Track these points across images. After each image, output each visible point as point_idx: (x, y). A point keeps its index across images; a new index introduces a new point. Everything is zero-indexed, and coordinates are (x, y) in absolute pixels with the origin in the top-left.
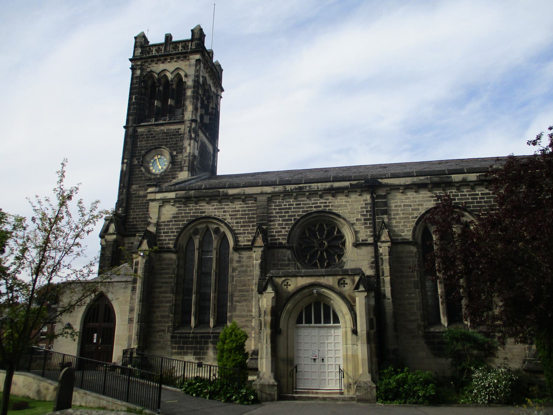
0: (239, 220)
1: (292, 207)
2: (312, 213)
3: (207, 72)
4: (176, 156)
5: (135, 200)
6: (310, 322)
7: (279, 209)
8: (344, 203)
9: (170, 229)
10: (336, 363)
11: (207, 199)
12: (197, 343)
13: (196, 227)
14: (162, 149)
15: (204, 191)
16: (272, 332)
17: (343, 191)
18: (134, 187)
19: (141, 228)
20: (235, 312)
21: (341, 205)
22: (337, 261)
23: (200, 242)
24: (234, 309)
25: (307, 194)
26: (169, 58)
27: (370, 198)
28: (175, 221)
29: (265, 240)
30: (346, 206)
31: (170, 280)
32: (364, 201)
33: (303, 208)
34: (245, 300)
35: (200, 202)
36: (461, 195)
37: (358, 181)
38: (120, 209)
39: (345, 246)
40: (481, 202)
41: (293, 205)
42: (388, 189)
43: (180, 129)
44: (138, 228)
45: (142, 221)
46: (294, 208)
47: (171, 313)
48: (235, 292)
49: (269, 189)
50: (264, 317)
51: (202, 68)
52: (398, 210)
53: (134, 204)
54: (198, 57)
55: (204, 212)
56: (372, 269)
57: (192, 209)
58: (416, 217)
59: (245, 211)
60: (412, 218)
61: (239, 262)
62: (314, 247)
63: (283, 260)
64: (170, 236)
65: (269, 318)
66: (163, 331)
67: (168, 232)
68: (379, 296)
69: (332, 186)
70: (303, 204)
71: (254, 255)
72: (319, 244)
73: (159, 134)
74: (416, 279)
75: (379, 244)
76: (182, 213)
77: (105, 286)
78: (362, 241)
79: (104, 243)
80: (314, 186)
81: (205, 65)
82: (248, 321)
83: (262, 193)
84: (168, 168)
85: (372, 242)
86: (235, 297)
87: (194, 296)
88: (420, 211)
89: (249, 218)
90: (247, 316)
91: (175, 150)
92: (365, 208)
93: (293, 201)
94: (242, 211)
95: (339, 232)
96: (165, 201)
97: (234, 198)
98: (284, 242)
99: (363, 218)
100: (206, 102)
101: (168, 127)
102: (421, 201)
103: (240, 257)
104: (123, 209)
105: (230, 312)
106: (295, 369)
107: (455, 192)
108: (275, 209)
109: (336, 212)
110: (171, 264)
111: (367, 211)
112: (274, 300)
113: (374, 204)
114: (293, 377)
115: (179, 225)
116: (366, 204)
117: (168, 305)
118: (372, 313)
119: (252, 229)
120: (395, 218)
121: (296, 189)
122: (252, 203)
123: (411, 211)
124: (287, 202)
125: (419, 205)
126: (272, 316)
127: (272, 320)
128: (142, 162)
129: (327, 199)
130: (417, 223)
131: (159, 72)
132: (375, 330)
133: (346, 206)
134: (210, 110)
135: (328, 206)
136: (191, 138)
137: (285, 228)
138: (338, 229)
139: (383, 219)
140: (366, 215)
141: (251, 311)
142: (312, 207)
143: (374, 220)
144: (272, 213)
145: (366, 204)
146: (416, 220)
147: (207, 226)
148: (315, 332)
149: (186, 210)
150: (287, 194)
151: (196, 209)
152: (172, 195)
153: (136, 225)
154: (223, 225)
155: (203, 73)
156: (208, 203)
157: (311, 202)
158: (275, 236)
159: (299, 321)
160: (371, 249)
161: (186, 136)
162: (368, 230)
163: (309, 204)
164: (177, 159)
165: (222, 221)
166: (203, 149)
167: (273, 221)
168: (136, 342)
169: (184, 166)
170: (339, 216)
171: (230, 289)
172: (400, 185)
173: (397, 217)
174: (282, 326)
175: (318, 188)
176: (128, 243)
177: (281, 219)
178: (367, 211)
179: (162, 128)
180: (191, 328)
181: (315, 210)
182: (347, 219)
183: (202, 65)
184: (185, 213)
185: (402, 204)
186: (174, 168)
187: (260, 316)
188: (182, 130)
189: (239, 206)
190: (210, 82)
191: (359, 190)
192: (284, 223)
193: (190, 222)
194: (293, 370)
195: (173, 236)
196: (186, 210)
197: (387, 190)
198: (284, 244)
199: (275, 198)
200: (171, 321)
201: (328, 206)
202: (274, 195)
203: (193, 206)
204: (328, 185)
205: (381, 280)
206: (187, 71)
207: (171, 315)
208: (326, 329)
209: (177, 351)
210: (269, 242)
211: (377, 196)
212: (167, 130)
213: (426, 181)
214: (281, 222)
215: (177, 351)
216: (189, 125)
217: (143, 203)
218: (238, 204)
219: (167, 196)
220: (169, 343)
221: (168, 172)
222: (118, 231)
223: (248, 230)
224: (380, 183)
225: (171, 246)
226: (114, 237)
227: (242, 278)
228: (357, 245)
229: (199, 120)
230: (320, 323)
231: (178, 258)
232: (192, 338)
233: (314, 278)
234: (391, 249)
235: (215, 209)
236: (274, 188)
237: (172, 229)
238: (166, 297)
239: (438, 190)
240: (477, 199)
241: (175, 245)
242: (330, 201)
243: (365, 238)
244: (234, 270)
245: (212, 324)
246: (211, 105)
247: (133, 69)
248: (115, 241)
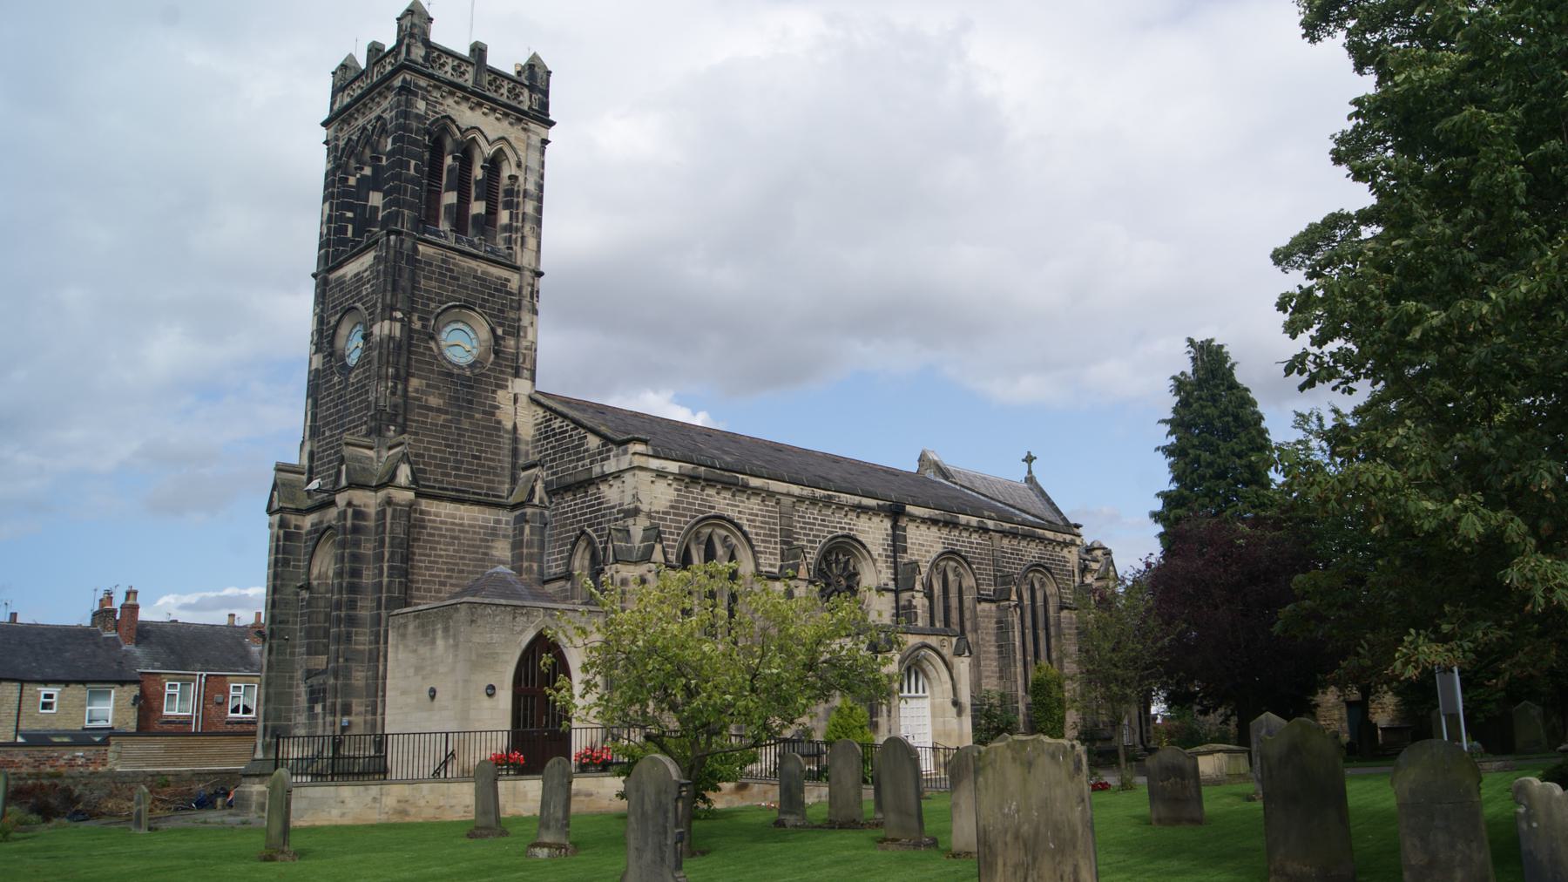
4: (503, 339)
5: (420, 415)
11: (719, 486)
14: (473, 314)
15: (718, 471)
18: (414, 382)
19: (435, 480)
26: (487, 104)
28: (675, 514)
33: (828, 527)
38: (392, 428)
41: (816, 519)
43: (508, 280)
44: (429, 480)
45: (437, 466)
46: (819, 525)
49: (796, 489)
53: (417, 421)
55: (713, 508)
57: (696, 499)
59: (764, 516)
73: (465, 275)
76: (682, 502)
77: (551, 616)
83: (788, 495)
89: (770, 529)
91: (501, 325)
92: (887, 540)
94: (764, 516)
96: (661, 474)
97: (756, 492)
99: (884, 553)
101: (485, 266)
104: (398, 429)
108: (799, 522)
109: (864, 541)
111: (888, 545)
115: (680, 522)
116: (887, 535)
121: (825, 497)
122: (772, 506)
129: (851, 519)
131: (464, 127)
142: (836, 527)
144: (795, 527)
145: (887, 535)
149: (688, 497)
150: (814, 501)
152: (673, 467)
153: (424, 471)
156: (718, 493)
163: (833, 522)
164: (504, 347)
165: (739, 527)
167: (797, 539)
169: (523, 368)
172: (919, 517)
178: (888, 545)
179: (473, 264)
184: (688, 503)
186: (500, 365)
202: (801, 499)
203: (698, 493)
206: (522, 154)
212: (483, 273)
216: (531, 282)
217: (436, 425)
223: (769, 548)
228: (881, 590)
235: (728, 505)
237: (670, 527)
243: (886, 581)
248: (411, 505)
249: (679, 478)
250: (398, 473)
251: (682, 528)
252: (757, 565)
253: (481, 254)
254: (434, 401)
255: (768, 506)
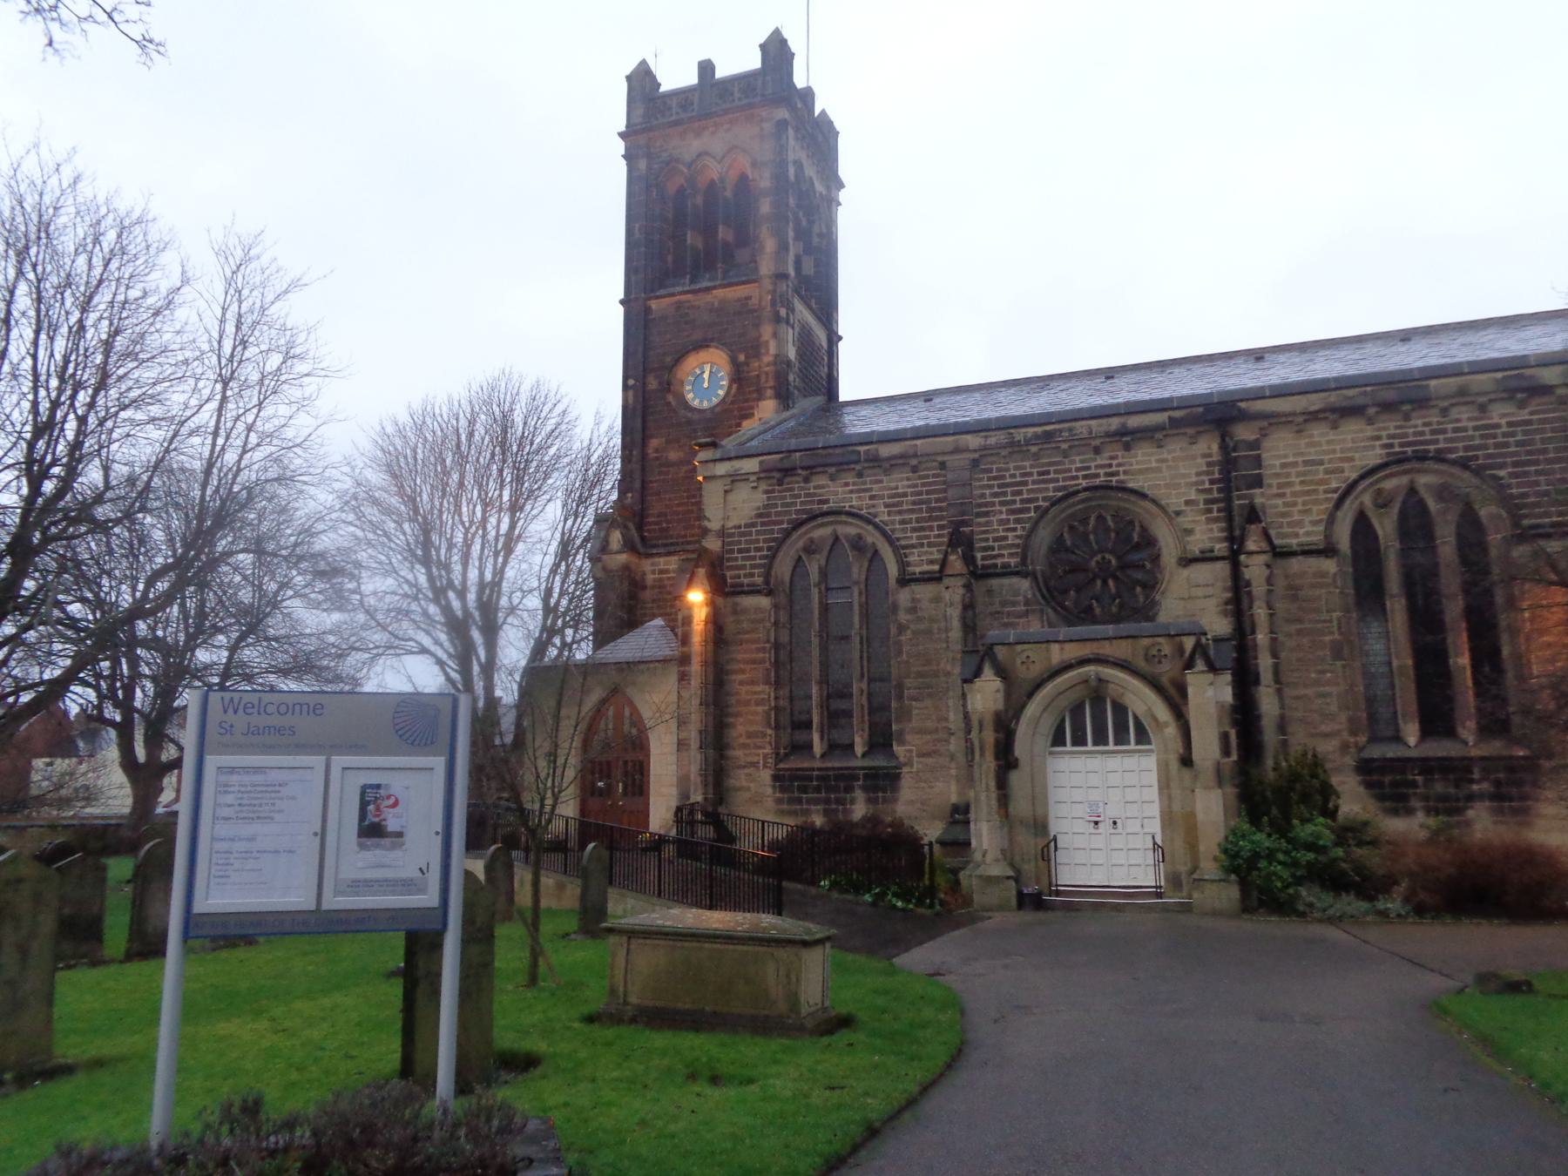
0: (906, 517)
1: (1030, 479)
2: (1077, 492)
3: (802, 147)
4: (747, 364)
5: (660, 473)
6: (1084, 743)
7: (999, 486)
8: (1154, 465)
9: (751, 542)
10: (1146, 830)
11: (832, 470)
12: (829, 790)
13: (811, 535)
16: (999, 766)
17: (1150, 434)
18: (654, 443)
20: (910, 720)
21: (1147, 469)
22: (1141, 599)
23: (820, 568)
24: (905, 714)
25: (1064, 446)
27: (1220, 448)
28: (763, 524)
29: (969, 559)
30: (1159, 470)
31: (761, 655)
32: (1204, 456)
33: (1057, 480)
34: (930, 695)
35: (814, 478)
36: (1456, 430)
37: (1188, 410)
38: (630, 495)
39: (1159, 566)
40: (1506, 445)
41: (1031, 474)
42: (1265, 423)
43: (749, 298)
44: (672, 537)
46: (1034, 482)
47: (769, 726)
48: (908, 676)
49: (973, 441)
50: (980, 731)
51: (792, 142)
52: (1288, 475)
54: (782, 113)
55: (826, 501)
56: (1226, 616)
57: (799, 496)
58: (1335, 491)
59: (920, 493)
60: (1326, 492)
61: (913, 610)
62: (1085, 570)
63: (1014, 604)
64: (754, 558)
65: (990, 736)
66: (754, 765)
67: (748, 550)
68: (1245, 681)
69: (1124, 425)
70: (1056, 472)
71: (947, 595)
72: (1097, 562)
74: (1337, 636)
75: (1242, 557)
76: (776, 505)
78: (1202, 552)
79: (600, 574)
80: (1081, 427)
81: (797, 130)
82: (939, 741)
83: (957, 450)
84: (728, 393)
85: (1226, 554)
86: (909, 689)
87: (815, 690)
88: (1346, 474)
89: (930, 510)
90: (937, 729)
92: (1208, 473)
93: (1032, 466)
94: (913, 494)
95: (1144, 529)
96: (735, 479)
97: (892, 464)
98: (1013, 561)
99: (1202, 497)
100: (804, 223)
102: (1350, 449)
103: (913, 600)
105: (899, 720)
106: (1052, 844)
107: (1439, 423)
110: (762, 620)
111: (1212, 482)
112: (1000, 696)
113: (1228, 464)
114: (1049, 860)
115: (772, 531)
117: (760, 709)
118: (1226, 721)
119: (938, 535)
120: (1283, 495)
121: (1036, 436)
122: (934, 476)
123: (1321, 476)
124: (1016, 468)
125: (1342, 460)
126: (996, 731)
127: (997, 742)
128: (669, 384)
129: (1112, 458)
130: (1339, 504)
132: (1234, 757)
133: (1159, 470)
134: (816, 240)
135: (1116, 474)
136: (777, 319)
137: (1015, 529)
138: (1142, 526)
139: (1251, 497)
140: (1209, 491)
141: (947, 720)
142: (1076, 478)
143: (1228, 500)
144: (983, 496)
145: (1209, 464)
146: (1336, 496)
147: (835, 531)
148: (1095, 763)
149: (785, 497)
151: (807, 495)
152: (751, 465)
154: (870, 528)
155: (795, 151)
156: (832, 478)
157: (1073, 467)
158: (993, 549)
159: (1058, 740)
160: (1223, 569)
161: (767, 311)
162: (1214, 526)
163: (1070, 470)
166: (806, 342)
167: (986, 514)
168: (700, 791)
170: (1143, 496)
171: (894, 671)
172: (1294, 414)
173: (1288, 491)
174: (1020, 749)
175: (1091, 433)
176: (653, 572)
177: (1004, 509)
178: (1212, 482)
179: (708, 298)
180: (813, 757)
181: (1084, 483)
182: (1163, 502)
183: (791, 132)
184: (783, 505)
185: (1300, 459)
187: (969, 732)
188: (755, 301)
189: (906, 483)
190: (810, 171)
191: (1191, 431)
192: (1012, 517)
193: (798, 525)
194: (1047, 845)
195: (761, 558)
196: (785, 497)
197: (1261, 429)
198: (1016, 566)
199: (990, 459)
200: (770, 743)
201: (1116, 474)
203: (802, 489)
204: (1115, 423)
205: (1250, 643)
207: (769, 732)
208: (1119, 756)
209: (785, 807)
210: (979, 563)
211: (1237, 442)
213: (1361, 401)
214: (1004, 517)
215: (785, 807)
218: (902, 480)
219: (741, 469)
220: (769, 791)
221: (732, 403)
222: (629, 546)
224: (1240, 410)
225: (759, 580)
226: (623, 558)
227: (921, 647)
228: (1187, 561)
229: (792, 272)
230: (1106, 743)
231: (776, 606)
232: (819, 778)
233: (1088, 644)
234: (1271, 572)
235: (851, 492)
236: (986, 437)
237: (757, 541)
238: (755, 693)
239: (1391, 420)
240: (1494, 436)
241: (767, 576)
242: (1120, 460)
243: (1208, 545)
244: (902, 629)
245: (859, 749)
246: (816, 229)
247: (628, 156)
249: (766, 472)
250: (611, 539)
251: (774, 540)
252: (903, 565)
253: (718, 283)
254: (673, 455)
255: (927, 477)
